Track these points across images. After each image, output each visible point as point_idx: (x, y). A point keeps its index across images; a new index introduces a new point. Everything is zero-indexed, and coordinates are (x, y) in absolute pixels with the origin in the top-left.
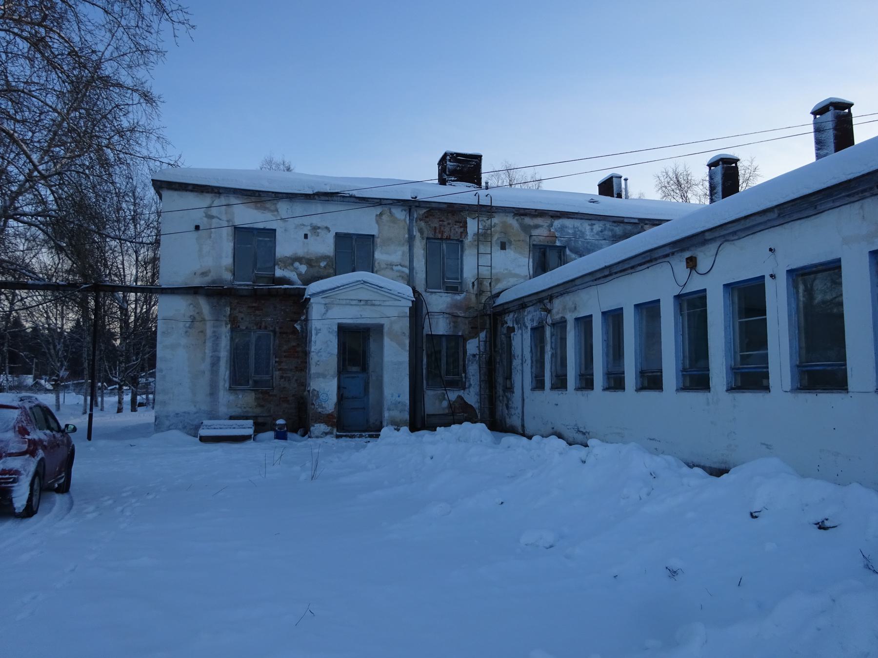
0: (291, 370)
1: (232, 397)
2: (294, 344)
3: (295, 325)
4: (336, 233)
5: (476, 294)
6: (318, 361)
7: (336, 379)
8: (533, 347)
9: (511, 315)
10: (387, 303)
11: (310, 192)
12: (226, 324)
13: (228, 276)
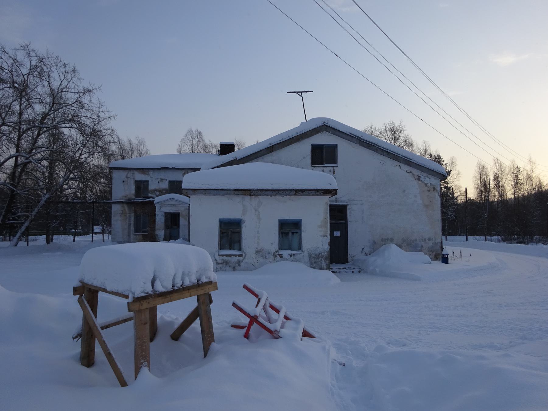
1: (135, 237)
4: (169, 181)
7: (164, 231)
10: (180, 205)
11: (159, 168)
12: (133, 213)
13: (134, 197)
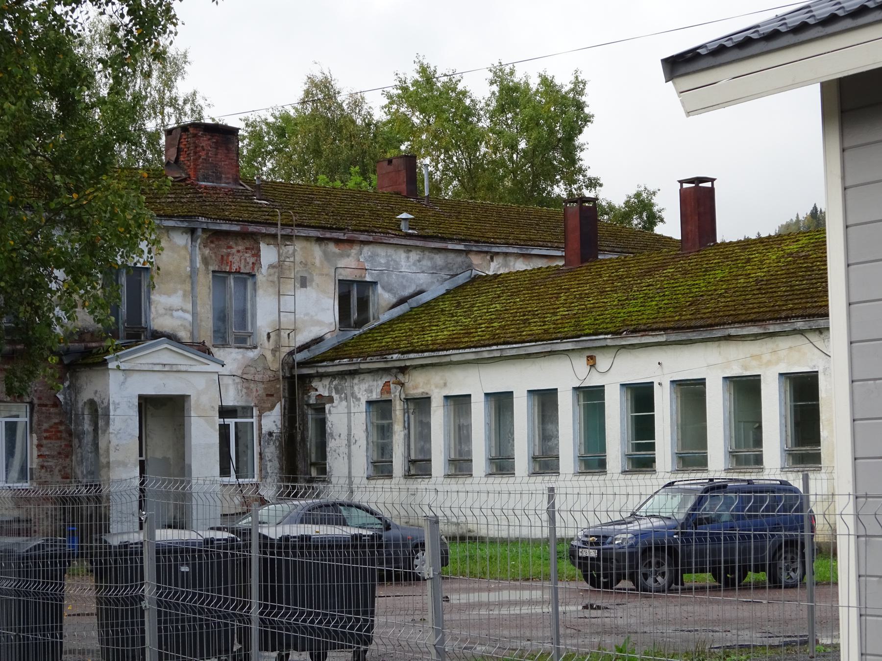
0: (53, 457)
2: (57, 421)
3: (57, 395)
5: (272, 350)
6: (118, 445)
7: (138, 468)
8: (369, 425)
9: (326, 382)
